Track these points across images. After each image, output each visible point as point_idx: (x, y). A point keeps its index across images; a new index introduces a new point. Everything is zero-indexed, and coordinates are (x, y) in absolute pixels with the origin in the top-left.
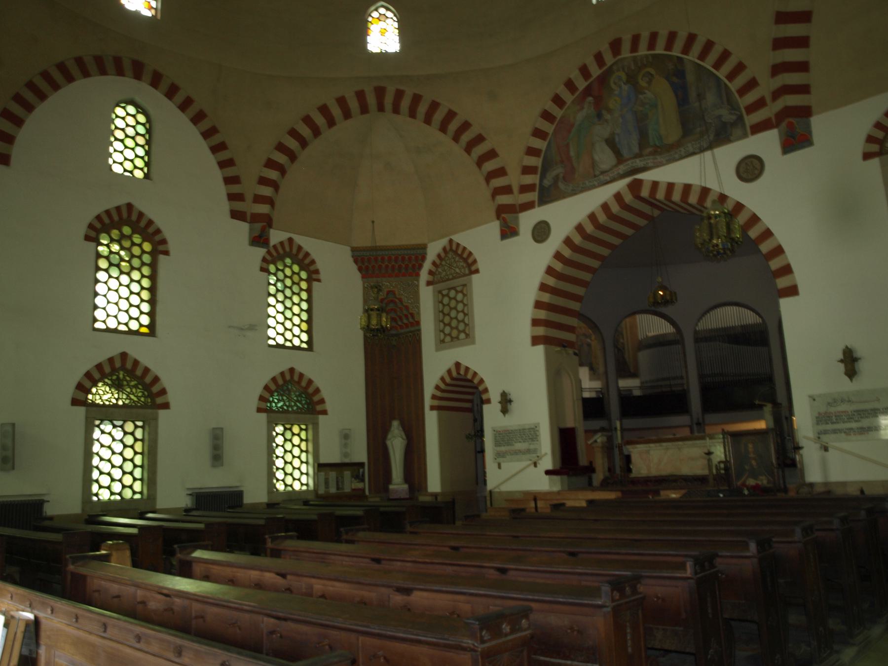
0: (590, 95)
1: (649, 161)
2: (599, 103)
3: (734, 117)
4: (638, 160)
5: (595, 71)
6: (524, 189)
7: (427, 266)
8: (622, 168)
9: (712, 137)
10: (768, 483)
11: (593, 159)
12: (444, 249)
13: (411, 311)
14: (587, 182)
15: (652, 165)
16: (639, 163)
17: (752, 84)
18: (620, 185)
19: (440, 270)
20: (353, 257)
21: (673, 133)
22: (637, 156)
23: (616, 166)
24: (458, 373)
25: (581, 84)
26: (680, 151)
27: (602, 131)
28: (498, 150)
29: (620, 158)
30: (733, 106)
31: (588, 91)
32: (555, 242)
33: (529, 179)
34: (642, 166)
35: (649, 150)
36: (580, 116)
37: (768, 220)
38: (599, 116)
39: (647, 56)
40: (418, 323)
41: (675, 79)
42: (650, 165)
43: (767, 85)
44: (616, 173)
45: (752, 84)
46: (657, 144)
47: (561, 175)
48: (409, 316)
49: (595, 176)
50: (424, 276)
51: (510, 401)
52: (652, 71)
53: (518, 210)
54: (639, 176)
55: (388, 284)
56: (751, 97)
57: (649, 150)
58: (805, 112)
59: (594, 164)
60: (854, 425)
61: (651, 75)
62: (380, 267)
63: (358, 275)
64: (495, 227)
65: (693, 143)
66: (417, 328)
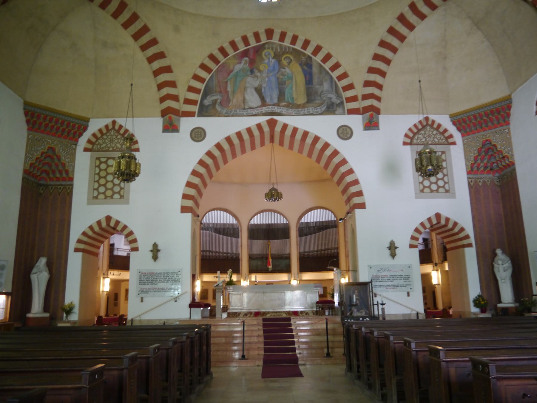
0: (247, 56)
1: (284, 110)
2: (252, 63)
3: (339, 102)
4: (276, 108)
5: (253, 43)
6: (188, 101)
7: (87, 135)
8: (265, 109)
9: (324, 109)
10: (365, 314)
11: (244, 97)
12: (107, 127)
13: (66, 168)
14: (238, 111)
15: (285, 113)
16: (276, 109)
17: (350, 87)
18: (263, 120)
19: (100, 141)
20: (24, 109)
21: (302, 99)
24: (108, 225)
25: (242, 48)
26: (304, 110)
27: (252, 82)
28: (173, 68)
29: (264, 103)
30: (339, 96)
31: (245, 54)
32: (208, 144)
33: (192, 96)
34: (278, 112)
35: (284, 104)
36: (238, 67)
37: (352, 163)
38: (252, 72)
39: (289, 47)
40: (71, 179)
42: (284, 113)
43: (359, 90)
44: (260, 111)
45: (350, 87)
46: (290, 102)
47: (219, 101)
48: (64, 172)
49: (244, 109)
50: (83, 141)
51: (158, 251)
52: (292, 58)
54: (275, 118)
55: (51, 141)
56: (350, 94)
57: (284, 104)
58: (377, 111)
59: (244, 101)
60: (390, 283)
61: (291, 60)
62: (47, 125)
63: (25, 127)
64: (159, 122)
65: (313, 108)
66: (69, 183)
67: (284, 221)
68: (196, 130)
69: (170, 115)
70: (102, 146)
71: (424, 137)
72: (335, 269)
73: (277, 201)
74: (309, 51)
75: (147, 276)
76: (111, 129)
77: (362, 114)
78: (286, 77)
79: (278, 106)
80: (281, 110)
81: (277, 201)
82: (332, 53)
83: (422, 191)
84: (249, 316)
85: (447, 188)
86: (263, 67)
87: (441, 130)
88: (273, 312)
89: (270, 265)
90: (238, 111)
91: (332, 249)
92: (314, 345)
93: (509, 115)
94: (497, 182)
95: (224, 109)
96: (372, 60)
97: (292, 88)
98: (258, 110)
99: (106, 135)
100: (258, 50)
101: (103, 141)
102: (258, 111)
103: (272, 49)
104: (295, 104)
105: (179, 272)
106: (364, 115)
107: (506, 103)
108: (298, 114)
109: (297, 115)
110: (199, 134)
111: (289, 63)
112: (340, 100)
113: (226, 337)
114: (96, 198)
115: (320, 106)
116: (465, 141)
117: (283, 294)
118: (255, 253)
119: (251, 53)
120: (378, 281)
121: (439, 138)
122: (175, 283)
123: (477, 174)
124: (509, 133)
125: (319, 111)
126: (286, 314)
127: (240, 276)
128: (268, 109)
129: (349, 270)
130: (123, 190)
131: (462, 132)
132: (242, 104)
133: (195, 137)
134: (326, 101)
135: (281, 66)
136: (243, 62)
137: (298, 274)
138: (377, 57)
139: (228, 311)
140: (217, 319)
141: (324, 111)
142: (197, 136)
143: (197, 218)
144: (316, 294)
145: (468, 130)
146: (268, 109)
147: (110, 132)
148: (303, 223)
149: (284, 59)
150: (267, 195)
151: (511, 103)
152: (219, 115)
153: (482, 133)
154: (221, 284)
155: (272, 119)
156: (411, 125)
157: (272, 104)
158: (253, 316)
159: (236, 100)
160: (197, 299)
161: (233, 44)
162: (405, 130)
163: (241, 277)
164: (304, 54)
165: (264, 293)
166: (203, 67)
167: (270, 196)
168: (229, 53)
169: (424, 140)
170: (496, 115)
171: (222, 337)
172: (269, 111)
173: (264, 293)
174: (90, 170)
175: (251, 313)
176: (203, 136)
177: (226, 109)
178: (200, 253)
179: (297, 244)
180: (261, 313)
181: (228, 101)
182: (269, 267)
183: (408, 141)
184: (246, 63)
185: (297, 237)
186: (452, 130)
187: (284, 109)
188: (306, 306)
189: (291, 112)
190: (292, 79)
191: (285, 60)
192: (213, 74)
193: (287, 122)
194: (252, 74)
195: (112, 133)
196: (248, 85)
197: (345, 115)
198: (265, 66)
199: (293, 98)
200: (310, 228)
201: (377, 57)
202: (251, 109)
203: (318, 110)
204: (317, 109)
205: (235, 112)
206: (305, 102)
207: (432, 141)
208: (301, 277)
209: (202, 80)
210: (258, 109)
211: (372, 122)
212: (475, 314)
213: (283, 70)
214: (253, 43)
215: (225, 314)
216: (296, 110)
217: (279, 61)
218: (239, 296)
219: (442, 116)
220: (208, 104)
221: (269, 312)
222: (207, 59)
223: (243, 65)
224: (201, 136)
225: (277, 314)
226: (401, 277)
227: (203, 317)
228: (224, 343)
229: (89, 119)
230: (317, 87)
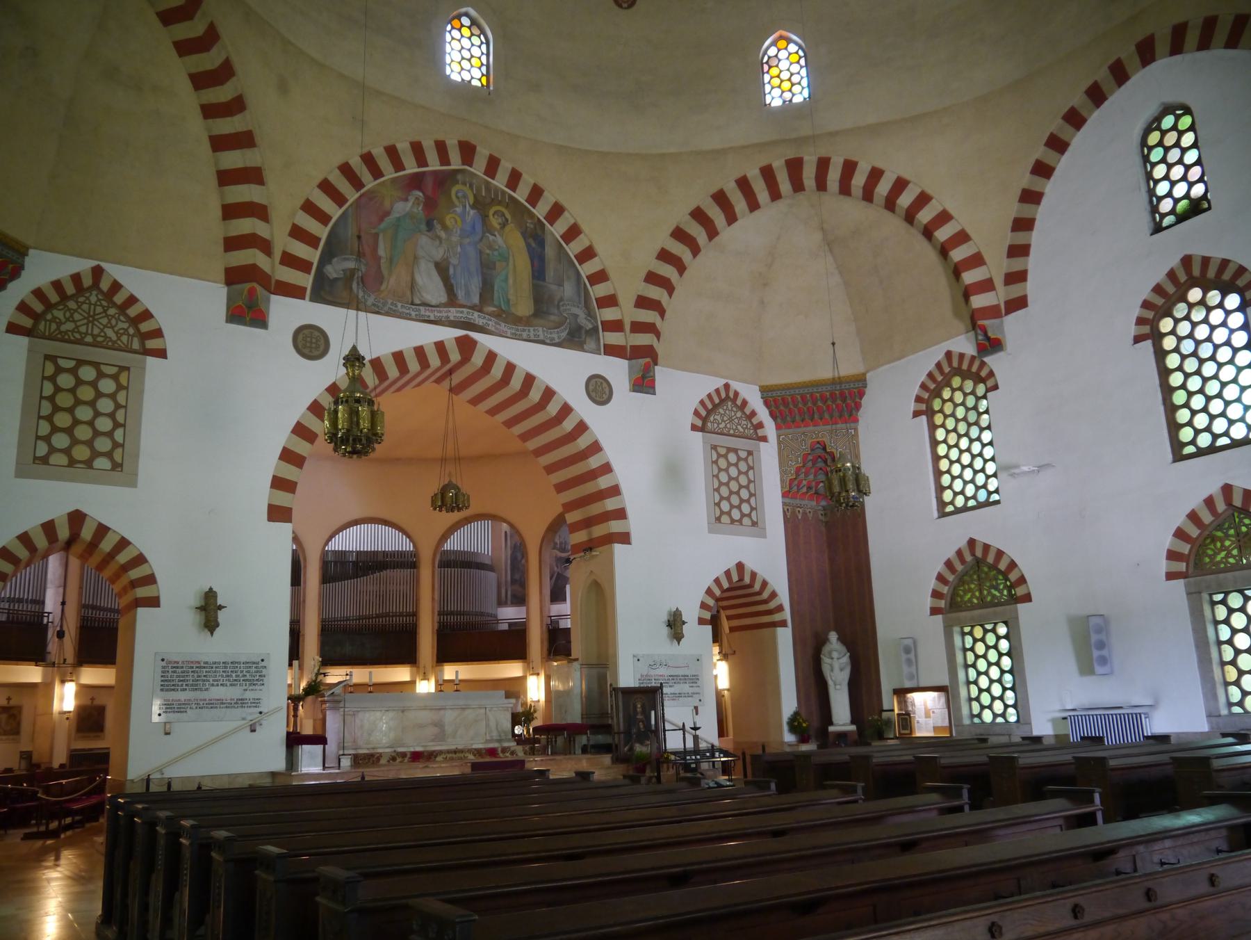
0: (420, 189)
1: (490, 323)
2: (430, 205)
3: (590, 326)
4: (476, 314)
5: (434, 165)
6: (289, 260)
8: (453, 313)
9: (564, 335)
14: (399, 305)
15: (493, 329)
16: (476, 318)
17: (610, 301)
18: (449, 334)
21: (524, 308)
22: (473, 308)
25: (411, 168)
26: (529, 331)
27: (428, 248)
28: (268, 176)
29: (452, 301)
30: (590, 315)
31: (415, 182)
33: (301, 250)
34: (481, 324)
35: (491, 309)
36: (401, 208)
38: (430, 225)
39: (503, 193)
41: (533, 245)
44: (445, 315)
45: (610, 301)
49: (412, 304)
52: (508, 216)
53: (272, 289)
54: (475, 335)
56: (609, 314)
57: (491, 309)
59: (413, 285)
61: (507, 220)
64: (216, 296)
65: (545, 329)
68: (306, 332)
69: (255, 285)
70: (63, 328)
71: (723, 421)
74: (540, 211)
75: (180, 670)
76: (90, 289)
77: (629, 359)
78: (496, 253)
80: (485, 321)
82: (584, 226)
83: (718, 519)
84: (401, 762)
85: (755, 520)
86: (452, 220)
87: (748, 411)
90: (399, 305)
93: (858, 406)
94: (822, 515)
95: (370, 296)
96: (656, 260)
97: (506, 280)
98: (440, 312)
99: (77, 302)
100: (444, 181)
101: (68, 314)
102: (441, 315)
103: (471, 186)
104: (513, 314)
105: (263, 660)
106: (634, 361)
107: (857, 386)
108: (517, 337)
110: (314, 340)
111: (503, 225)
112: (592, 323)
114: (44, 460)
116: (781, 437)
119: (429, 182)
121: (745, 426)
122: (254, 687)
123: (796, 498)
124: (856, 436)
125: (555, 336)
126: (475, 755)
127: (418, 672)
128: (461, 315)
130: (119, 450)
131: (779, 420)
132: (409, 293)
133: (305, 347)
134: (568, 321)
135: (487, 228)
136: (412, 200)
138: (664, 256)
141: (564, 339)
142: (308, 345)
145: (788, 419)
146: (461, 315)
147: (87, 295)
149: (493, 215)
151: (866, 387)
152: (358, 306)
153: (811, 428)
155: (466, 337)
156: (703, 395)
157: (469, 304)
159: (395, 280)
161: (392, 152)
162: (695, 403)
164: (532, 215)
165: (403, 711)
166: (326, 187)
168: (385, 173)
169: (722, 426)
170: (839, 402)
173: (403, 711)
174: (27, 385)
175: (403, 755)
177: (373, 297)
178: (79, 612)
180: (425, 754)
181: (380, 279)
183: (699, 423)
184: (419, 204)
186: (763, 414)
187: (491, 320)
189: (505, 329)
190: (506, 260)
191: (496, 217)
192: (347, 209)
193: (495, 349)
194: (429, 230)
195: (93, 299)
196: (421, 253)
198: (456, 222)
199: (508, 301)
201: (664, 256)
202: (427, 308)
203: (553, 336)
205: (394, 308)
206: (531, 313)
207: (734, 430)
209: (323, 218)
210: (441, 309)
211: (646, 377)
212: (790, 745)
213: (491, 238)
214: (434, 165)
215: (348, 758)
217: (484, 218)
219: (750, 385)
220: (335, 276)
222: (337, 172)
223: (407, 207)
224: (317, 348)
225: (458, 755)
226: (686, 679)
229: (27, 249)
230: (553, 287)
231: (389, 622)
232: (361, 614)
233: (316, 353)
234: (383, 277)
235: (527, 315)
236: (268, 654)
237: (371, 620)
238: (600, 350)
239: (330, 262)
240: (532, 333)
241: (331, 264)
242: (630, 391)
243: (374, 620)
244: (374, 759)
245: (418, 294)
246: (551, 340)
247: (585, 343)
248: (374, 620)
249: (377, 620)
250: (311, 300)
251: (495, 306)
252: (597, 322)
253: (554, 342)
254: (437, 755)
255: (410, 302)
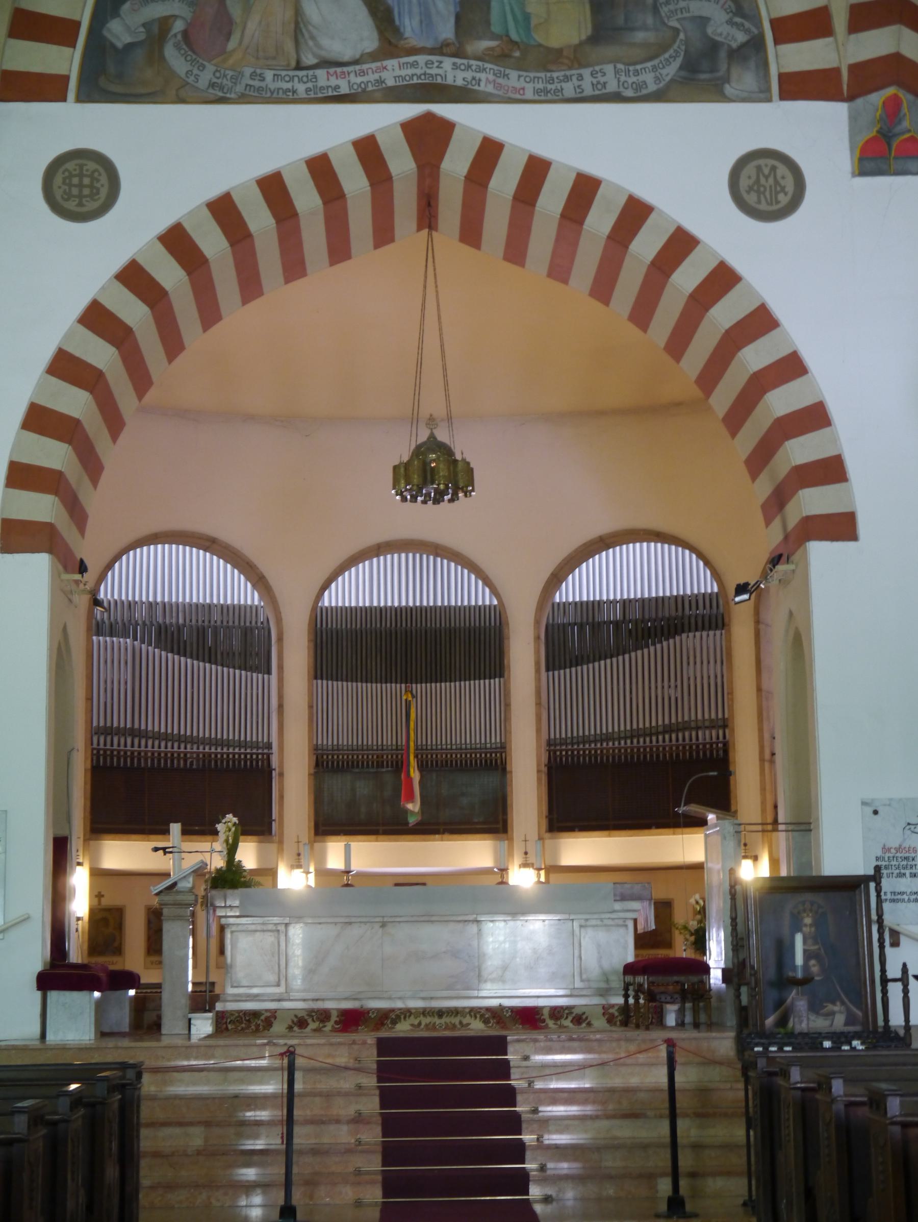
1: (483, 76)
3: (741, 37)
4: (448, 62)
9: (671, 70)
14: (269, 75)
15: (490, 89)
22: (441, 50)
23: (374, 57)
26: (580, 77)
34: (460, 82)
44: (372, 77)
46: (514, 36)
47: (179, 26)
49: (299, 67)
54: (444, 110)
65: (620, 66)
67: (483, 597)
68: (70, 165)
72: (711, 817)
73: (451, 501)
77: (850, 98)
79: (459, 53)
80: (469, 75)
81: (451, 501)
84: (315, 1030)
88: (425, 1012)
89: (411, 798)
90: (269, 75)
91: (697, 728)
92: (612, 1162)
95: (202, 68)
98: (363, 73)
102: (365, 79)
104: (540, 45)
106: (860, 101)
108: (550, 96)
109: (543, 98)
110: (86, 181)
112: (747, 31)
113: (207, 1124)
115: (651, 59)
117: (473, 928)
118: (344, 741)
120: (908, 872)
126: (486, 1022)
127: (273, 847)
128: (410, 71)
129: (775, 822)
132: (289, 46)
133: (68, 196)
134: (682, 36)
137: (541, 838)
139: (219, 1007)
140: (165, 1041)
141: (672, 81)
142: (75, 191)
143: (78, 577)
144: (622, 931)
146: (410, 71)
148: (566, 605)
150: (401, 473)
154: (188, 884)
155: (429, 117)
157: (429, 44)
158: (334, 1030)
160: (76, 953)
163: (280, 850)
165: (383, 925)
167: (416, 479)
171: (191, 1124)
172: (415, 81)
173: (383, 925)
175: (323, 1016)
176: (104, 192)
177: (210, 68)
179: (538, 704)
182: (410, 806)
185: (538, 671)
187: (485, 69)
188: (578, 984)
189: (518, 85)
193: (497, 134)
197: (769, 100)
199: (527, 17)
200: (596, 627)
202: (332, 70)
203: (641, 78)
204: (637, 73)
205: (256, 83)
206: (584, 37)
208: (556, 853)
210: (365, 67)
211: (895, 135)
215: (207, 1019)
216: (542, 75)
218: (270, 938)
220: (127, 39)
221: (407, 1013)
224: (94, 193)
227: (103, 1034)
228: (199, 1153)
231: (691, 739)
232: (635, 726)
233: (91, 206)
234: (231, 22)
235: (576, 41)
236: (6, 811)
237: (654, 738)
238: (768, 90)
239: (115, 13)
240: (588, 81)
241: (118, 15)
242: (854, 175)
243: (660, 738)
244: (259, 1022)
245: (311, 43)
246: (636, 90)
247: (728, 82)
248: (660, 738)
249: (667, 737)
250: (79, 99)
251: (494, 37)
252: (759, 24)
253: (644, 92)
254: (398, 1017)
255: (293, 64)
